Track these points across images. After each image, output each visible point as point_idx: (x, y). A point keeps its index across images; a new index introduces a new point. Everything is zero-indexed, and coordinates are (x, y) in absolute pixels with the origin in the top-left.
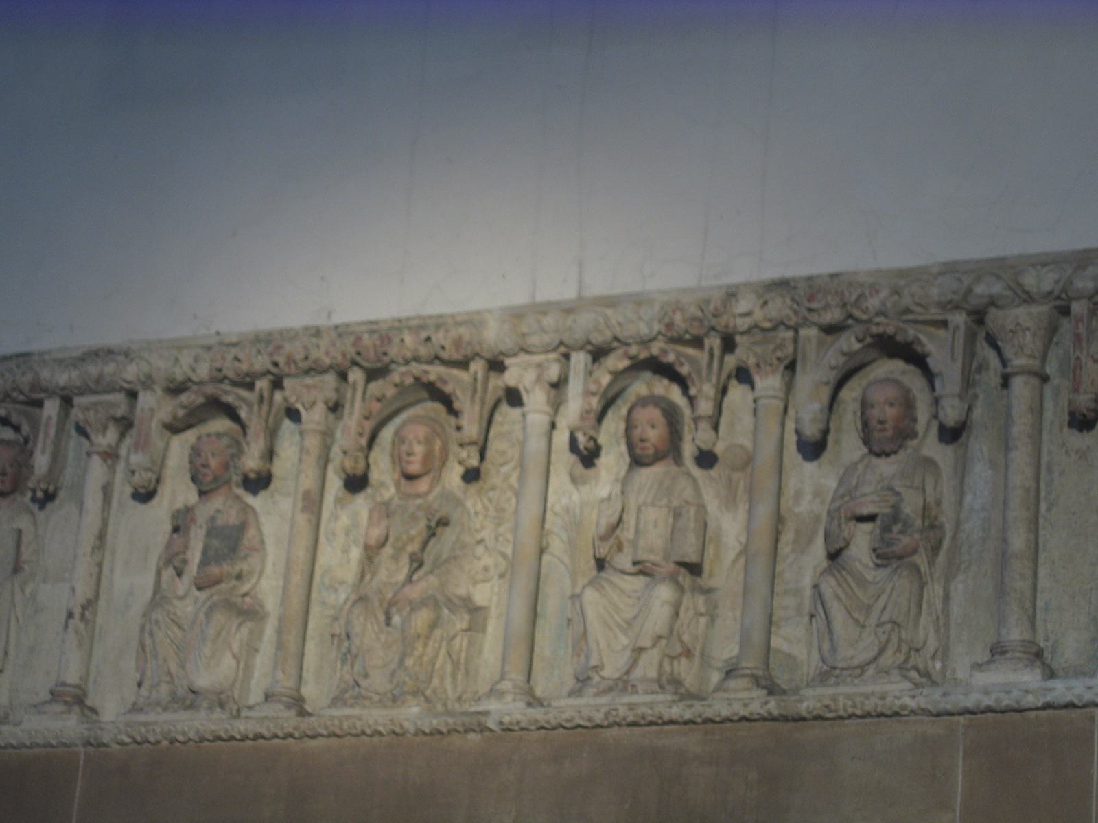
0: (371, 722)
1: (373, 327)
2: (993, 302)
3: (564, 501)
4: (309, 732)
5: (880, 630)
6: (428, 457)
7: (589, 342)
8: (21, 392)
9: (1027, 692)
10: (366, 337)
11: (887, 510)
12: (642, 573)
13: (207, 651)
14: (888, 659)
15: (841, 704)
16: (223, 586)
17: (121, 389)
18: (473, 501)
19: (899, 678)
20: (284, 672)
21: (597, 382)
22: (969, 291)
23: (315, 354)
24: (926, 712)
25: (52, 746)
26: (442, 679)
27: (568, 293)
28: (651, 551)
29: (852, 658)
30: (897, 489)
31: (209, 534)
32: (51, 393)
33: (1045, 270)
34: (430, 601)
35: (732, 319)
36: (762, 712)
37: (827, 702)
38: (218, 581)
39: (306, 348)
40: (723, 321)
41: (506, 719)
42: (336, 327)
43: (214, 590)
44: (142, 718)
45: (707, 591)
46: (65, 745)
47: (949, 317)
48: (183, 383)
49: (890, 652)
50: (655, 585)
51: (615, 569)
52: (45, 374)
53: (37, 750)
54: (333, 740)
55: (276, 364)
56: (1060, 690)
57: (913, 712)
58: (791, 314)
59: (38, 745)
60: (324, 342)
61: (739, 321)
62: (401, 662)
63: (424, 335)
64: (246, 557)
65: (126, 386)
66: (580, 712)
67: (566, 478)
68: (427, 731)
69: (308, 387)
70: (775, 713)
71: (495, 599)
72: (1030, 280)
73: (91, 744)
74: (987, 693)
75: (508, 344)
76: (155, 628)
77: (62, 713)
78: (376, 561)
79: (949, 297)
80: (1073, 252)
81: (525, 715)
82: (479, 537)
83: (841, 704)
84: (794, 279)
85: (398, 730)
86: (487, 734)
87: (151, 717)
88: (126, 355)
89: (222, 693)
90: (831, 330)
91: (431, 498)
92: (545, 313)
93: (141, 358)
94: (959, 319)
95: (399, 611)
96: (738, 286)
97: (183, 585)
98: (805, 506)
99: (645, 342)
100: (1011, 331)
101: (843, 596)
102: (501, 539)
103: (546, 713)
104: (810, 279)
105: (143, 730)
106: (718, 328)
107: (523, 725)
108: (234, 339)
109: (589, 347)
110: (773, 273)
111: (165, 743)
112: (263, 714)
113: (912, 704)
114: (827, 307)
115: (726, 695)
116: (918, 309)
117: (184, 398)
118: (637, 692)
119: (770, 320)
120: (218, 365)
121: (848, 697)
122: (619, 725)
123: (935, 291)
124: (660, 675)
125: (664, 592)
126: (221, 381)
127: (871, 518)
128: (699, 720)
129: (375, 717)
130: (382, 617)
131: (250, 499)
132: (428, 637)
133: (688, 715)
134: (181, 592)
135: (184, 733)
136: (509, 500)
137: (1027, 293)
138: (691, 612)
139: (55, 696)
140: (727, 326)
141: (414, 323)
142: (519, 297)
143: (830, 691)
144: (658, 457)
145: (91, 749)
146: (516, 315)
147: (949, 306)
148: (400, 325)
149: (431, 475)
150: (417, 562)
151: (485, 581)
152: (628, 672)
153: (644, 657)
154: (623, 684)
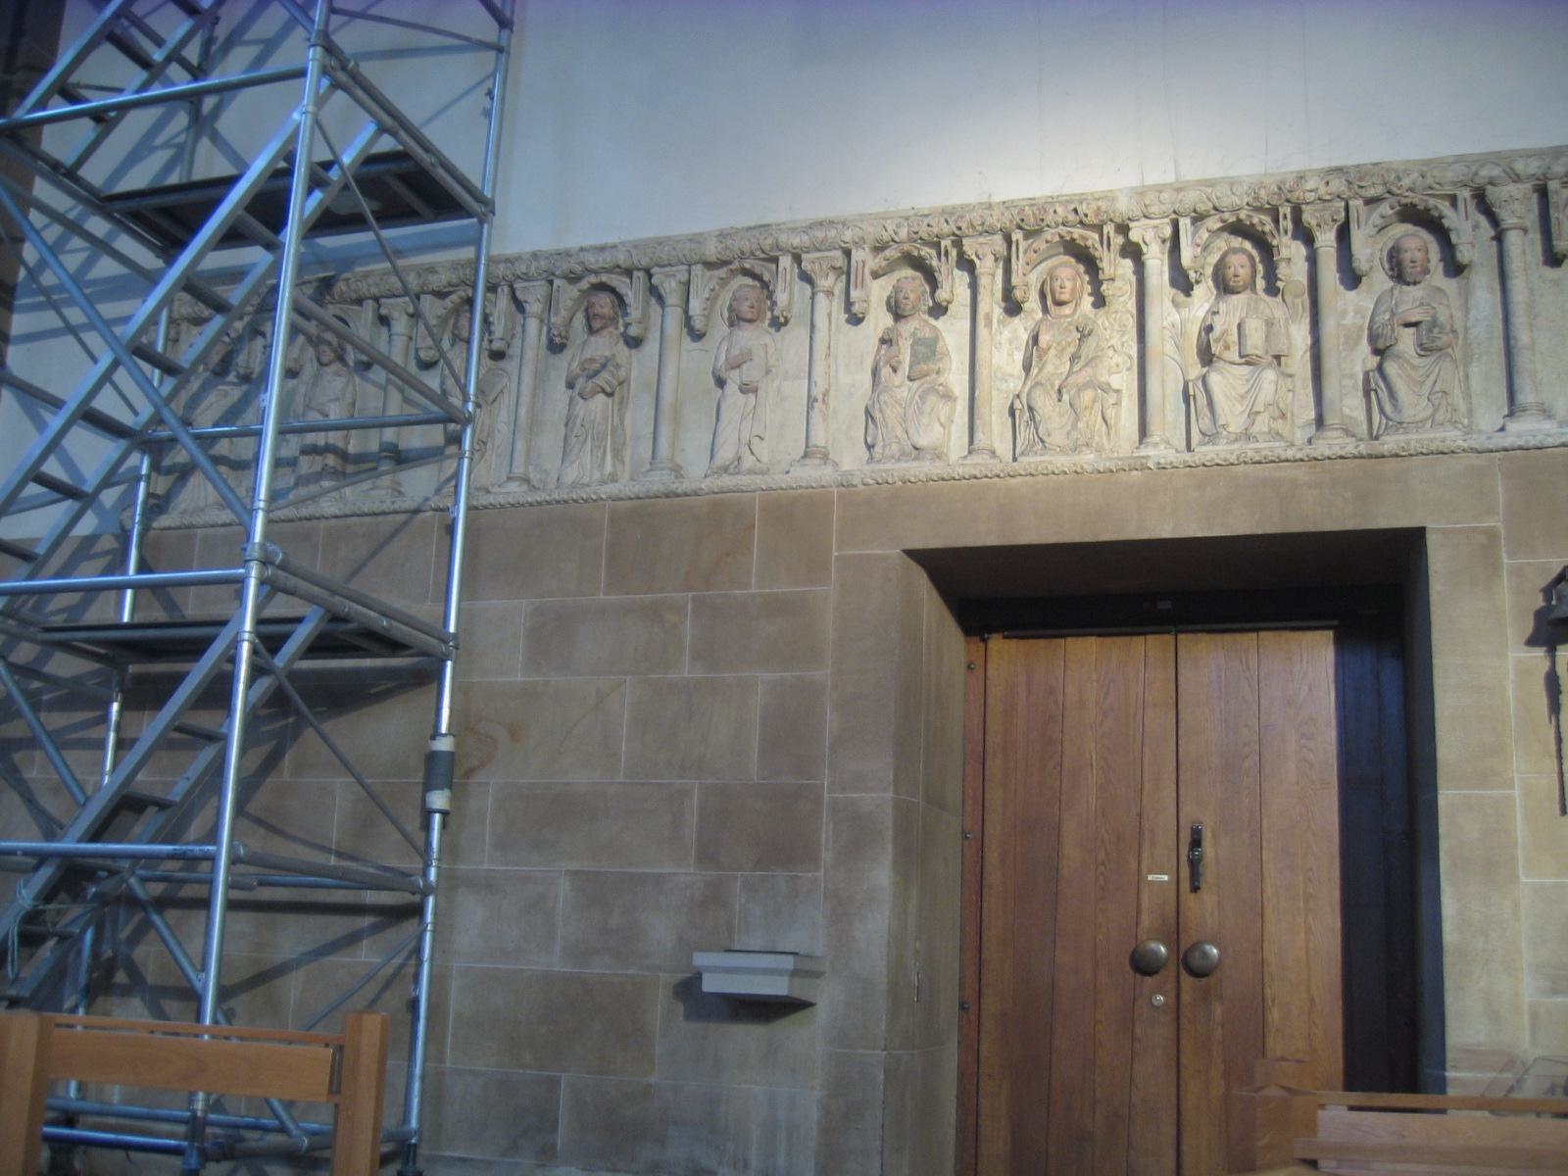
0: (1059, 465)
1: (1032, 202)
3: (1170, 319)
4: (1011, 473)
5: (1432, 397)
6: (1074, 289)
7: (1195, 211)
8: (763, 252)
9: (1549, 436)
10: (1027, 208)
11: (1429, 319)
12: (1248, 363)
13: (925, 420)
14: (1440, 417)
15: (1412, 447)
16: (928, 378)
17: (842, 248)
18: (1102, 320)
19: (1452, 428)
20: (984, 434)
21: (1200, 238)
22: (1476, 174)
23: (989, 221)
24: (1473, 450)
25: (812, 487)
26: (1100, 436)
27: (1171, 178)
28: (1256, 348)
29: (1415, 416)
30: (1434, 305)
33: (1531, 159)
34: (1088, 385)
35: (1301, 194)
36: (1355, 452)
37: (1403, 444)
39: (981, 217)
40: (1294, 197)
41: (1162, 461)
42: (1004, 203)
43: (922, 381)
44: (881, 466)
45: (1291, 376)
46: (823, 487)
47: (1458, 193)
48: (888, 242)
51: (1225, 361)
52: (783, 239)
53: (799, 491)
54: (1029, 478)
55: (960, 228)
57: (1464, 450)
58: (1346, 189)
59: (801, 487)
60: (996, 213)
61: (1308, 195)
62: (1074, 426)
63: (1072, 207)
64: (940, 359)
65: (843, 245)
66: (1217, 455)
67: (1171, 304)
68: (1102, 470)
69: (981, 244)
70: (1365, 453)
71: (1125, 384)
72: (1520, 167)
73: (843, 486)
74: (1519, 436)
75: (1138, 213)
76: (884, 406)
77: (820, 465)
78: (1044, 359)
79: (1461, 178)
80: (1551, 148)
81: (1177, 458)
82: (1110, 344)
83: (1412, 447)
84: (1345, 166)
85: (1079, 470)
86: (1146, 471)
87: (889, 466)
88: (844, 224)
89: (936, 449)
90: (1370, 202)
91: (1076, 317)
92: (1161, 192)
93: (855, 226)
94: (1465, 194)
95: (1068, 392)
96: (1305, 171)
99: (1235, 210)
100: (1505, 201)
101: (1403, 375)
102: (1125, 345)
103: (1194, 456)
104: (1358, 166)
105: (884, 474)
106: (1292, 200)
107: (1175, 465)
108: (926, 212)
109: (1193, 214)
112: (975, 462)
113: (1465, 445)
115: (1325, 442)
116: (1437, 186)
117: (887, 253)
118: (1257, 441)
119: (1330, 194)
120: (916, 230)
121: (1418, 441)
122: (1245, 463)
123: (1450, 175)
125: (1270, 375)
126: (915, 241)
127: (1415, 324)
128: (1306, 459)
129: (1063, 462)
130: (1055, 396)
131: (932, 321)
132: (1092, 408)
133: (1299, 456)
134: (897, 383)
135: (915, 476)
136: (1128, 319)
137: (1516, 175)
138: (1284, 389)
139: (806, 455)
140: (1298, 199)
141: (1060, 199)
142: (1135, 182)
143: (1403, 437)
144: (1244, 288)
146: (1141, 192)
147: (1459, 184)
148: (1052, 201)
149: (1074, 302)
150: (1074, 358)
152: (1246, 429)
153: (1259, 418)
154: (1247, 436)
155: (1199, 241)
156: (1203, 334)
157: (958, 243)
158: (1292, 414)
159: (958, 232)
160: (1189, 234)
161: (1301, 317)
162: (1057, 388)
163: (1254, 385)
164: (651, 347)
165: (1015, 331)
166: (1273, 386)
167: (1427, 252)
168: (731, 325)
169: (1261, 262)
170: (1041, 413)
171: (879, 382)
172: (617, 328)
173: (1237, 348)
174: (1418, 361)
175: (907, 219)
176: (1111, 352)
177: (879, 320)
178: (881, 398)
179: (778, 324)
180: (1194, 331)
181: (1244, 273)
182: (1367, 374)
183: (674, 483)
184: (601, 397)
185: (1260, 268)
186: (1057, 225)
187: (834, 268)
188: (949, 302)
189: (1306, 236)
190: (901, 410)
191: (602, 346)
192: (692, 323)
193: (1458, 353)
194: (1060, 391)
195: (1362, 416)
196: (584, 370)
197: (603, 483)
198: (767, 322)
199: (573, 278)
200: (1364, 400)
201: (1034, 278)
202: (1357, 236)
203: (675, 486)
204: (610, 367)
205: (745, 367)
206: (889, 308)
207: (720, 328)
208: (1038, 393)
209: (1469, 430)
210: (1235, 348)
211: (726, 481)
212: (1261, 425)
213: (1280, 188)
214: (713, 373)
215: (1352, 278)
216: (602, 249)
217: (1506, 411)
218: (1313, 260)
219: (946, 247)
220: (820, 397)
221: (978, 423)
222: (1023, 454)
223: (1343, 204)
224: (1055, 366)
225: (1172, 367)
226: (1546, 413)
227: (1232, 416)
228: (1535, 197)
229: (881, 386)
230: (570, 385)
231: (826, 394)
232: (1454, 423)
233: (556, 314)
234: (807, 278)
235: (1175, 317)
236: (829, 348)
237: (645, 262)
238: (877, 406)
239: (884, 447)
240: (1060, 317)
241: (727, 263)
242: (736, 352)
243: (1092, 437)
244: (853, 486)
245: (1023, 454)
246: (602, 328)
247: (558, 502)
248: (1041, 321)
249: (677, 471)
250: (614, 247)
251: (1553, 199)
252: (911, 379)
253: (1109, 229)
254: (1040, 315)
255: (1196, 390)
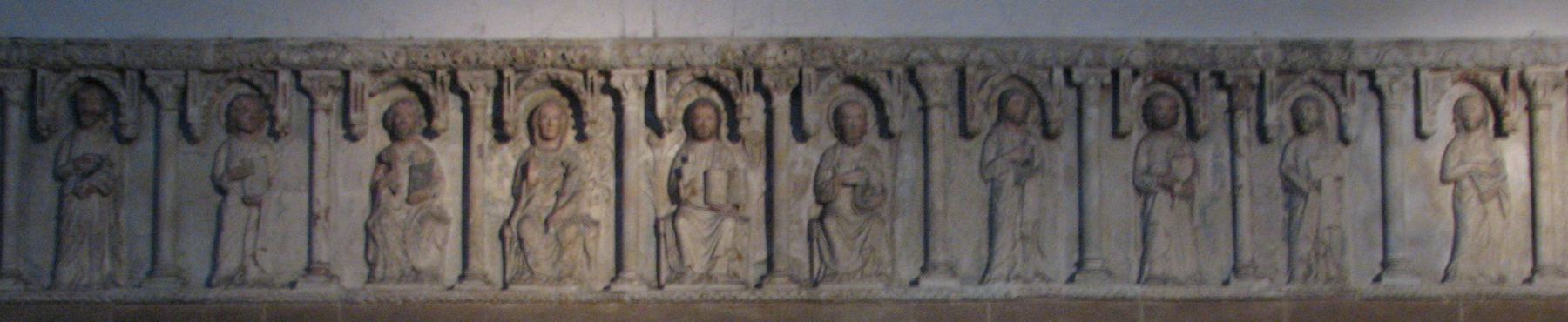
2: (921, 63)
6: (559, 127)
14: (867, 270)
18: (584, 153)
21: (674, 90)
23: (484, 58)
27: (646, 32)
31: (411, 169)
32: (284, 66)
34: (571, 221)
38: (425, 198)
40: (757, 61)
41: (637, 296)
42: (497, 42)
43: (420, 205)
44: (382, 287)
45: (746, 220)
46: (329, 303)
49: (869, 264)
50: (723, 220)
52: (283, 55)
54: (517, 305)
55: (455, 62)
56: (972, 291)
60: (490, 50)
63: (560, 52)
69: (476, 78)
70: (806, 298)
72: (944, 53)
74: (930, 290)
75: (618, 62)
82: (591, 177)
88: (344, 46)
90: (823, 71)
94: (899, 71)
95: (555, 225)
97: (397, 202)
98: (799, 170)
99: (704, 67)
108: (424, 43)
110: (781, 31)
111: (400, 302)
112: (468, 288)
113: (888, 296)
114: (824, 58)
121: (851, 290)
123: (887, 55)
124: (728, 271)
125: (729, 224)
126: (413, 69)
127: (854, 186)
129: (549, 291)
130: (542, 228)
131: (427, 143)
133: (752, 298)
139: (309, 270)
141: (550, 43)
144: (710, 136)
145: (347, 306)
146: (622, 43)
148: (543, 43)
150: (559, 194)
151: (597, 204)
152: (709, 270)
153: (719, 262)
154: (708, 277)
155: (673, 93)
156: (673, 176)
157: (453, 74)
158: (748, 256)
159: (454, 65)
160: (665, 83)
161: (759, 162)
162: (543, 219)
163: (716, 232)
164: (146, 146)
165: (503, 158)
166: (731, 234)
167: (865, 116)
168: (229, 131)
169: (726, 109)
170: (530, 243)
171: (378, 206)
172: (106, 121)
173: (702, 194)
174: (853, 218)
175: (405, 48)
176: (591, 185)
177: (377, 139)
178: (383, 221)
179: (275, 135)
180: (665, 170)
181: (710, 124)
182: (811, 222)
183: (180, 292)
184: (95, 197)
185: (724, 115)
186: (546, 66)
187: (332, 87)
188: (444, 130)
189: (767, 95)
190: (400, 233)
191: (92, 143)
192: (191, 130)
193: (885, 212)
194: (546, 223)
195: (804, 259)
196: (77, 168)
197: (105, 286)
198: (265, 132)
199: (59, 70)
200: (808, 244)
201: (523, 109)
202: (809, 102)
203: (182, 295)
204: (106, 168)
205: (248, 180)
206: (385, 126)
207: (219, 134)
208: (526, 226)
209: (890, 280)
210: (701, 195)
211: (233, 293)
212: (721, 268)
213: (744, 53)
214: (213, 177)
215: (801, 134)
216: (92, 44)
217: (921, 263)
218: (769, 113)
219: (442, 77)
220: (322, 215)
221: (472, 250)
222: (513, 280)
223: (795, 71)
224: (542, 200)
225: (646, 203)
226: (952, 271)
227: (696, 257)
228: (956, 77)
229: (381, 208)
230: (60, 178)
231: (327, 211)
232: (879, 275)
233: (43, 105)
234: (302, 90)
235: (648, 155)
236: (329, 166)
237: (139, 63)
238: (378, 229)
239: (385, 267)
240: (546, 151)
241: (226, 71)
242: (236, 163)
243: (574, 268)
244: (357, 303)
245: (513, 279)
246: (93, 124)
247: (59, 303)
248: (527, 151)
249: (180, 276)
250: (105, 44)
251: (969, 83)
252: (408, 201)
253: (592, 73)
254: (526, 144)
255: (666, 228)
